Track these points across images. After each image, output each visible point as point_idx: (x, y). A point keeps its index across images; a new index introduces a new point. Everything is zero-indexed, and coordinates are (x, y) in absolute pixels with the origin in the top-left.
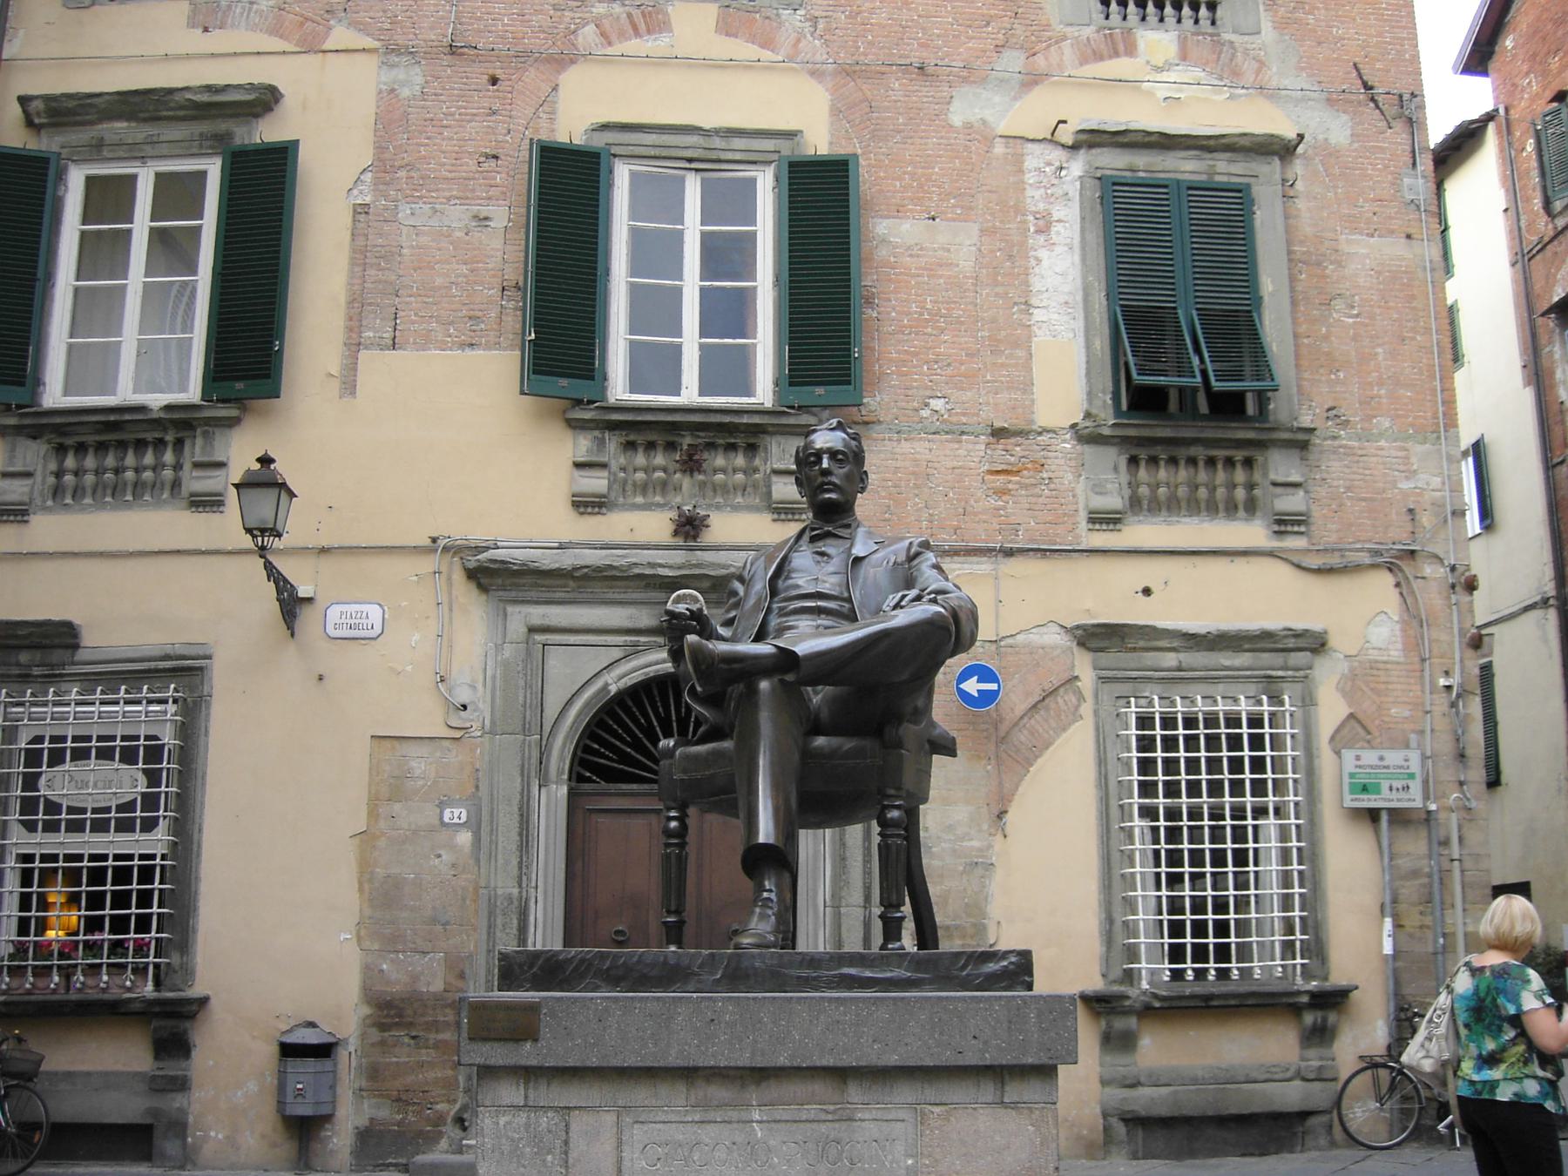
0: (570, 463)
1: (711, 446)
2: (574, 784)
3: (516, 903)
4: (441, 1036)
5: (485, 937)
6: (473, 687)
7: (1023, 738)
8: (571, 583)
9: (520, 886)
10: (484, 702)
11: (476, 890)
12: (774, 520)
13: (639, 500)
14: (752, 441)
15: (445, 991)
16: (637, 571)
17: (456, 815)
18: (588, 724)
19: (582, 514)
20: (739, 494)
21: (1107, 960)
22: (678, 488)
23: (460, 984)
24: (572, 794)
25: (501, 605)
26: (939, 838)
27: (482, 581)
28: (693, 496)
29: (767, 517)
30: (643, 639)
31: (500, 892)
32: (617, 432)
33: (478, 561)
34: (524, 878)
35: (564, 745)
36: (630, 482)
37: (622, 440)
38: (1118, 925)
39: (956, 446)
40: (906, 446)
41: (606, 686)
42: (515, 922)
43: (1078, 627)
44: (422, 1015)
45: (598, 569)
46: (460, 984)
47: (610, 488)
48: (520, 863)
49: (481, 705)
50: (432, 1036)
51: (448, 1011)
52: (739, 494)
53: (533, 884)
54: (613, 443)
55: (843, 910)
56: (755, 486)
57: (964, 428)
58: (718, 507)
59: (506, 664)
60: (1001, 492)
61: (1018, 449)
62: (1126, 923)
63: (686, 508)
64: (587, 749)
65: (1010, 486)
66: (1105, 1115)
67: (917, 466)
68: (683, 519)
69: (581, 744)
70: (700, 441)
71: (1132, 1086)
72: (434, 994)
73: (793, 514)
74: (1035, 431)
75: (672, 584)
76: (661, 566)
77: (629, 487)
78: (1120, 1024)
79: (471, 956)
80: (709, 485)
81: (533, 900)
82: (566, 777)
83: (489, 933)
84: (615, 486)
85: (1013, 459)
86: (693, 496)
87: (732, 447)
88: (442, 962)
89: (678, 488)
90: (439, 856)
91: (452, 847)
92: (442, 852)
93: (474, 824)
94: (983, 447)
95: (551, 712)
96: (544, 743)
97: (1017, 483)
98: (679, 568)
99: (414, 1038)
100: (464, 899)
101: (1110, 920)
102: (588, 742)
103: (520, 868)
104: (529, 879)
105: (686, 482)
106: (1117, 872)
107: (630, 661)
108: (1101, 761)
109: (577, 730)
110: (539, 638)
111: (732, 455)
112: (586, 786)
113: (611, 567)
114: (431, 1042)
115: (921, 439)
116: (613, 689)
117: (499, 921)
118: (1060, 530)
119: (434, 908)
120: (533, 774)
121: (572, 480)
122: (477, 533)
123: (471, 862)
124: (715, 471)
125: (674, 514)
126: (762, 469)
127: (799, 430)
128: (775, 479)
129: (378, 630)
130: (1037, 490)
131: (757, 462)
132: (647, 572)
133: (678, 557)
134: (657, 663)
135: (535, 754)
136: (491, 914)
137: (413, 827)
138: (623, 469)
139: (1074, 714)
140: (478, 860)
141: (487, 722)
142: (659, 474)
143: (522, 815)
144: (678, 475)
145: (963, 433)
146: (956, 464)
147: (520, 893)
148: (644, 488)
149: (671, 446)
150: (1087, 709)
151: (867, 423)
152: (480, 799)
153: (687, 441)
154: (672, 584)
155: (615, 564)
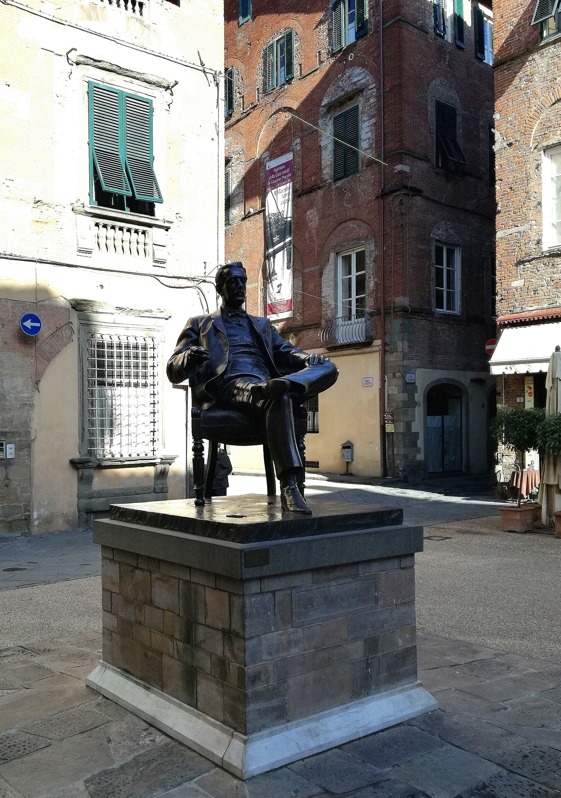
7: (47, 348)
21: (80, 447)
26: (9, 392)
38: (86, 430)
43: (73, 300)
62: (89, 431)
66: (79, 511)
71: (91, 498)
78: (87, 472)
101: (83, 429)
106: (86, 409)
108: (81, 360)
139: (69, 339)
150: (75, 337)
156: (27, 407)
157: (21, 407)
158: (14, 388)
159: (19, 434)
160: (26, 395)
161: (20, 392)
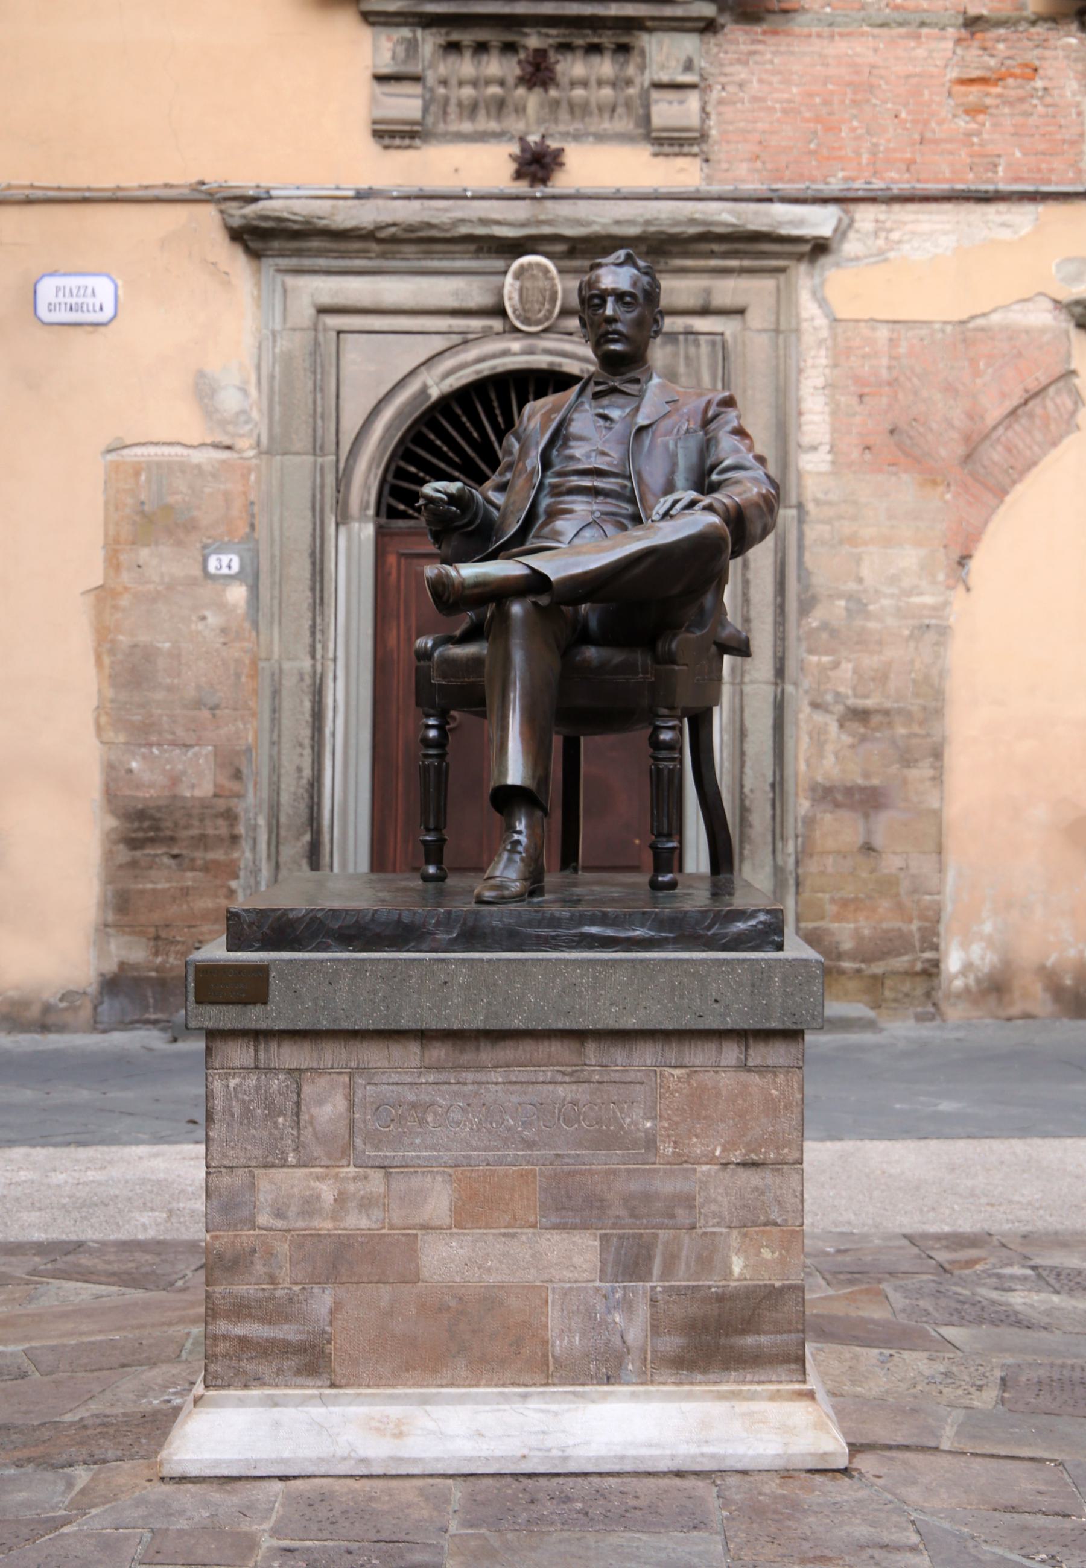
0: (368, 74)
1: (565, 47)
2: (383, 520)
3: (308, 680)
4: (211, 856)
5: (267, 724)
6: (244, 391)
8: (374, 247)
9: (313, 657)
10: (260, 411)
11: (254, 663)
12: (656, 155)
13: (467, 127)
14: (624, 40)
15: (215, 796)
16: (464, 230)
17: (225, 562)
18: (402, 441)
19: (386, 147)
20: (606, 116)
22: (520, 110)
23: (235, 786)
24: (381, 535)
25: (279, 277)
27: (251, 244)
28: (540, 121)
29: (649, 149)
30: (476, 324)
31: (287, 665)
32: (434, 30)
33: (244, 217)
34: (319, 646)
35: (369, 469)
36: (453, 101)
37: (442, 40)
39: (913, 44)
40: (842, 46)
41: (424, 391)
42: (307, 705)
44: (187, 827)
45: (411, 228)
46: (235, 786)
47: (425, 110)
48: (313, 627)
49: (255, 414)
50: (199, 854)
51: (220, 822)
52: (606, 116)
53: (331, 655)
54: (429, 42)
55: (747, 689)
56: (628, 105)
57: (925, 17)
58: (577, 137)
59: (287, 359)
60: (974, 111)
61: (1001, 46)
63: (533, 138)
64: (400, 474)
65: (988, 101)
67: (857, 73)
68: (528, 156)
69: (393, 467)
70: (551, 41)
72: (201, 799)
73: (681, 145)
74: (1026, 19)
75: (514, 248)
76: (498, 223)
77: (452, 109)
79: (249, 750)
80: (564, 106)
81: (331, 676)
82: (371, 512)
83: (273, 720)
84: (433, 108)
85: (992, 62)
86: (540, 121)
87: (594, 49)
88: (211, 758)
89: (520, 110)
90: (203, 618)
91: (221, 606)
92: (208, 613)
93: (251, 576)
94: (950, 45)
95: (351, 424)
96: (342, 465)
97: (999, 96)
98: (523, 225)
99: (175, 857)
100: (238, 676)
102: (402, 464)
103: (313, 634)
104: (325, 648)
105: (533, 100)
107: (457, 353)
109: (386, 448)
110: (334, 322)
111: (595, 60)
112: (401, 524)
113: (430, 225)
114: (199, 862)
115: (862, 34)
116: (435, 393)
117: (287, 704)
118: (1057, 164)
119: (199, 688)
120: (327, 508)
121: (374, 100)
122: (243, 180)
123: (247, 625)
124: (573, 84)
125: (515, 149)
126: (638, 81)
127: (689, 25)
128: (655, 95)
129: (108, 312)
130: (1026, 107)
131: (631, 70)
132: (481, 231)
133: (520, 211)
134: (494, 356)
135: (330, 480)
136: (276, 693)
137: (167, 579)
138: (444, 82)
140: (255, 624)
141: (264, 440)
142: (494, 90)
143: (313, 564)
144: (521, 91)
145: (923, 24)
146: (911, 69)
147: (314, 666)
148: (472, 109)
149: (509, 48)
151: (785, 12)
152: (257, 541)
153: (533, 41)
154: (514, 248)
155: (434, 221)
156: (931, 637)
157: (911, 636)
158: (893, 580)
159: (908, 716)
160: (928, 600)
161: (909, 593)
